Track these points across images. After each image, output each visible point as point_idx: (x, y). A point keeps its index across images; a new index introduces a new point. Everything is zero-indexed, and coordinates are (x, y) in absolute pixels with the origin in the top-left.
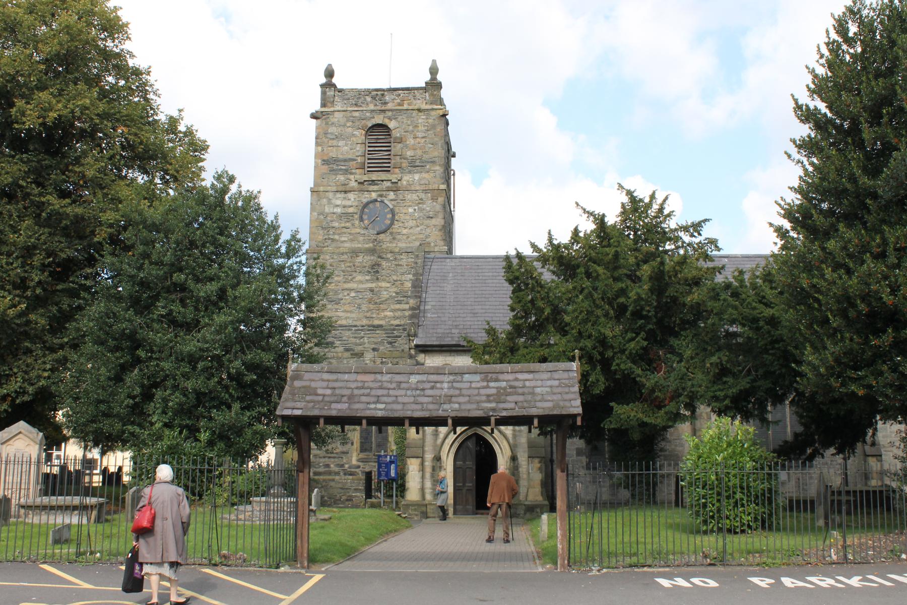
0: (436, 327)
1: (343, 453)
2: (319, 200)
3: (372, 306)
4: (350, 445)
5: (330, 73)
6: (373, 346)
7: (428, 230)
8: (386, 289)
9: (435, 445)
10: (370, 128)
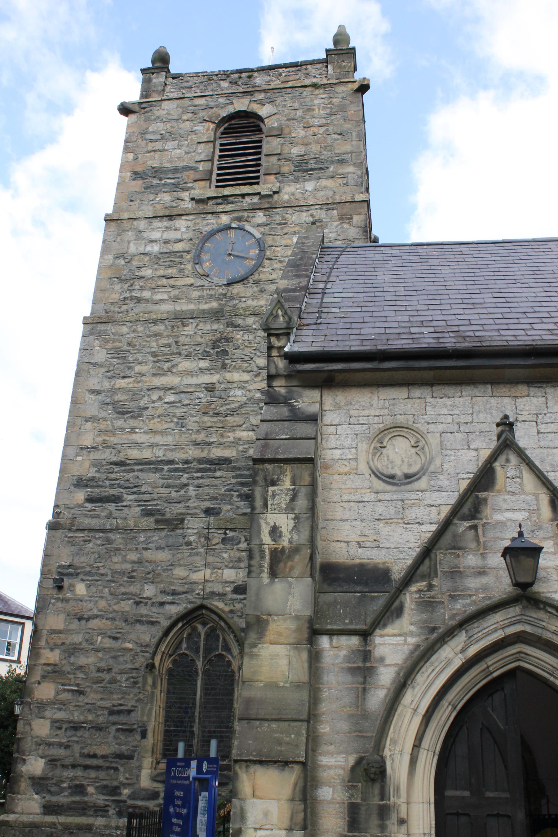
1: (120, 756)
2: (119, 235)
3: (208, 420)
4: (138, 737)
6: (207, 504)
8: (241, 385)
10: (224, 120)
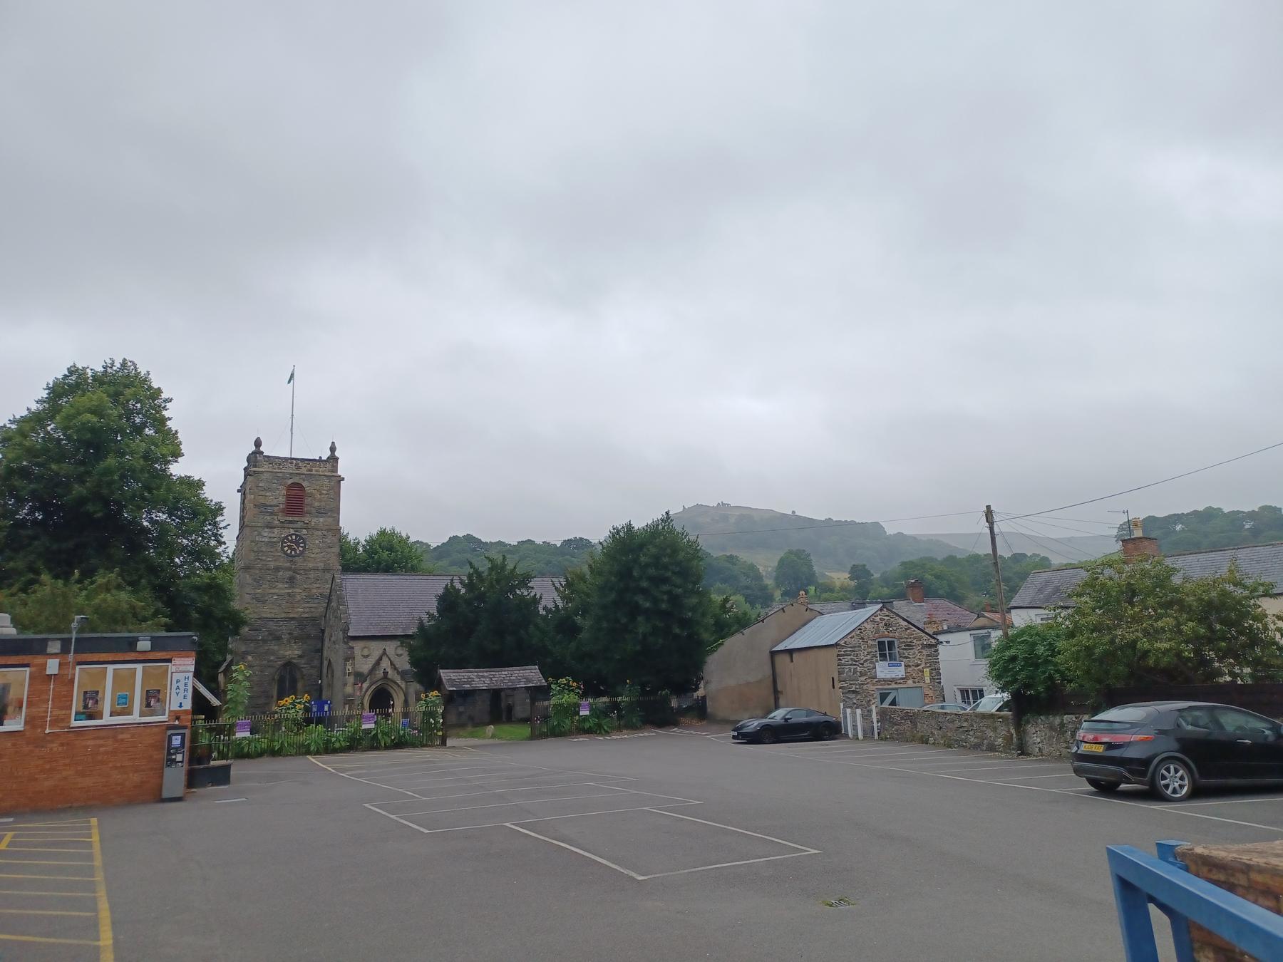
5: (258, 443)
6: (289, 632)
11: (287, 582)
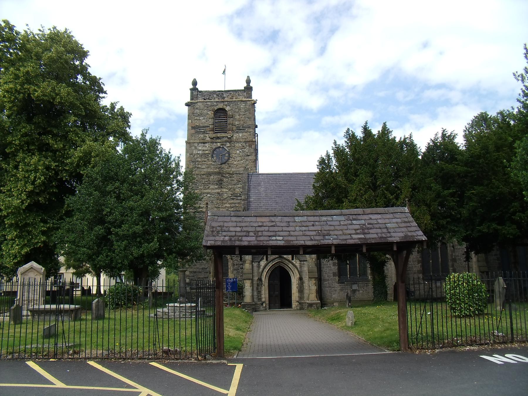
0: (257, 209)
5: (195, 83)
7: (247, 162)
8: (226, 192)
9: (258, 273)
11: (217, 184)
